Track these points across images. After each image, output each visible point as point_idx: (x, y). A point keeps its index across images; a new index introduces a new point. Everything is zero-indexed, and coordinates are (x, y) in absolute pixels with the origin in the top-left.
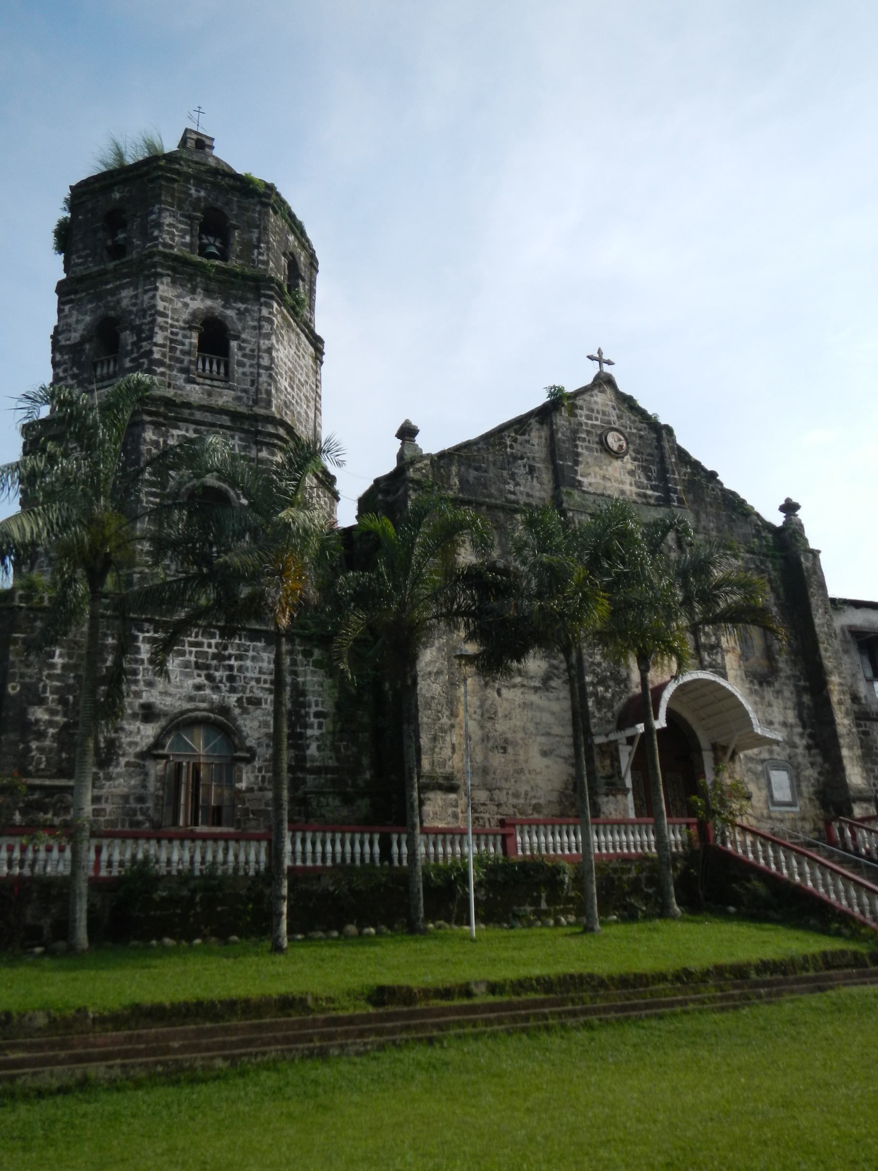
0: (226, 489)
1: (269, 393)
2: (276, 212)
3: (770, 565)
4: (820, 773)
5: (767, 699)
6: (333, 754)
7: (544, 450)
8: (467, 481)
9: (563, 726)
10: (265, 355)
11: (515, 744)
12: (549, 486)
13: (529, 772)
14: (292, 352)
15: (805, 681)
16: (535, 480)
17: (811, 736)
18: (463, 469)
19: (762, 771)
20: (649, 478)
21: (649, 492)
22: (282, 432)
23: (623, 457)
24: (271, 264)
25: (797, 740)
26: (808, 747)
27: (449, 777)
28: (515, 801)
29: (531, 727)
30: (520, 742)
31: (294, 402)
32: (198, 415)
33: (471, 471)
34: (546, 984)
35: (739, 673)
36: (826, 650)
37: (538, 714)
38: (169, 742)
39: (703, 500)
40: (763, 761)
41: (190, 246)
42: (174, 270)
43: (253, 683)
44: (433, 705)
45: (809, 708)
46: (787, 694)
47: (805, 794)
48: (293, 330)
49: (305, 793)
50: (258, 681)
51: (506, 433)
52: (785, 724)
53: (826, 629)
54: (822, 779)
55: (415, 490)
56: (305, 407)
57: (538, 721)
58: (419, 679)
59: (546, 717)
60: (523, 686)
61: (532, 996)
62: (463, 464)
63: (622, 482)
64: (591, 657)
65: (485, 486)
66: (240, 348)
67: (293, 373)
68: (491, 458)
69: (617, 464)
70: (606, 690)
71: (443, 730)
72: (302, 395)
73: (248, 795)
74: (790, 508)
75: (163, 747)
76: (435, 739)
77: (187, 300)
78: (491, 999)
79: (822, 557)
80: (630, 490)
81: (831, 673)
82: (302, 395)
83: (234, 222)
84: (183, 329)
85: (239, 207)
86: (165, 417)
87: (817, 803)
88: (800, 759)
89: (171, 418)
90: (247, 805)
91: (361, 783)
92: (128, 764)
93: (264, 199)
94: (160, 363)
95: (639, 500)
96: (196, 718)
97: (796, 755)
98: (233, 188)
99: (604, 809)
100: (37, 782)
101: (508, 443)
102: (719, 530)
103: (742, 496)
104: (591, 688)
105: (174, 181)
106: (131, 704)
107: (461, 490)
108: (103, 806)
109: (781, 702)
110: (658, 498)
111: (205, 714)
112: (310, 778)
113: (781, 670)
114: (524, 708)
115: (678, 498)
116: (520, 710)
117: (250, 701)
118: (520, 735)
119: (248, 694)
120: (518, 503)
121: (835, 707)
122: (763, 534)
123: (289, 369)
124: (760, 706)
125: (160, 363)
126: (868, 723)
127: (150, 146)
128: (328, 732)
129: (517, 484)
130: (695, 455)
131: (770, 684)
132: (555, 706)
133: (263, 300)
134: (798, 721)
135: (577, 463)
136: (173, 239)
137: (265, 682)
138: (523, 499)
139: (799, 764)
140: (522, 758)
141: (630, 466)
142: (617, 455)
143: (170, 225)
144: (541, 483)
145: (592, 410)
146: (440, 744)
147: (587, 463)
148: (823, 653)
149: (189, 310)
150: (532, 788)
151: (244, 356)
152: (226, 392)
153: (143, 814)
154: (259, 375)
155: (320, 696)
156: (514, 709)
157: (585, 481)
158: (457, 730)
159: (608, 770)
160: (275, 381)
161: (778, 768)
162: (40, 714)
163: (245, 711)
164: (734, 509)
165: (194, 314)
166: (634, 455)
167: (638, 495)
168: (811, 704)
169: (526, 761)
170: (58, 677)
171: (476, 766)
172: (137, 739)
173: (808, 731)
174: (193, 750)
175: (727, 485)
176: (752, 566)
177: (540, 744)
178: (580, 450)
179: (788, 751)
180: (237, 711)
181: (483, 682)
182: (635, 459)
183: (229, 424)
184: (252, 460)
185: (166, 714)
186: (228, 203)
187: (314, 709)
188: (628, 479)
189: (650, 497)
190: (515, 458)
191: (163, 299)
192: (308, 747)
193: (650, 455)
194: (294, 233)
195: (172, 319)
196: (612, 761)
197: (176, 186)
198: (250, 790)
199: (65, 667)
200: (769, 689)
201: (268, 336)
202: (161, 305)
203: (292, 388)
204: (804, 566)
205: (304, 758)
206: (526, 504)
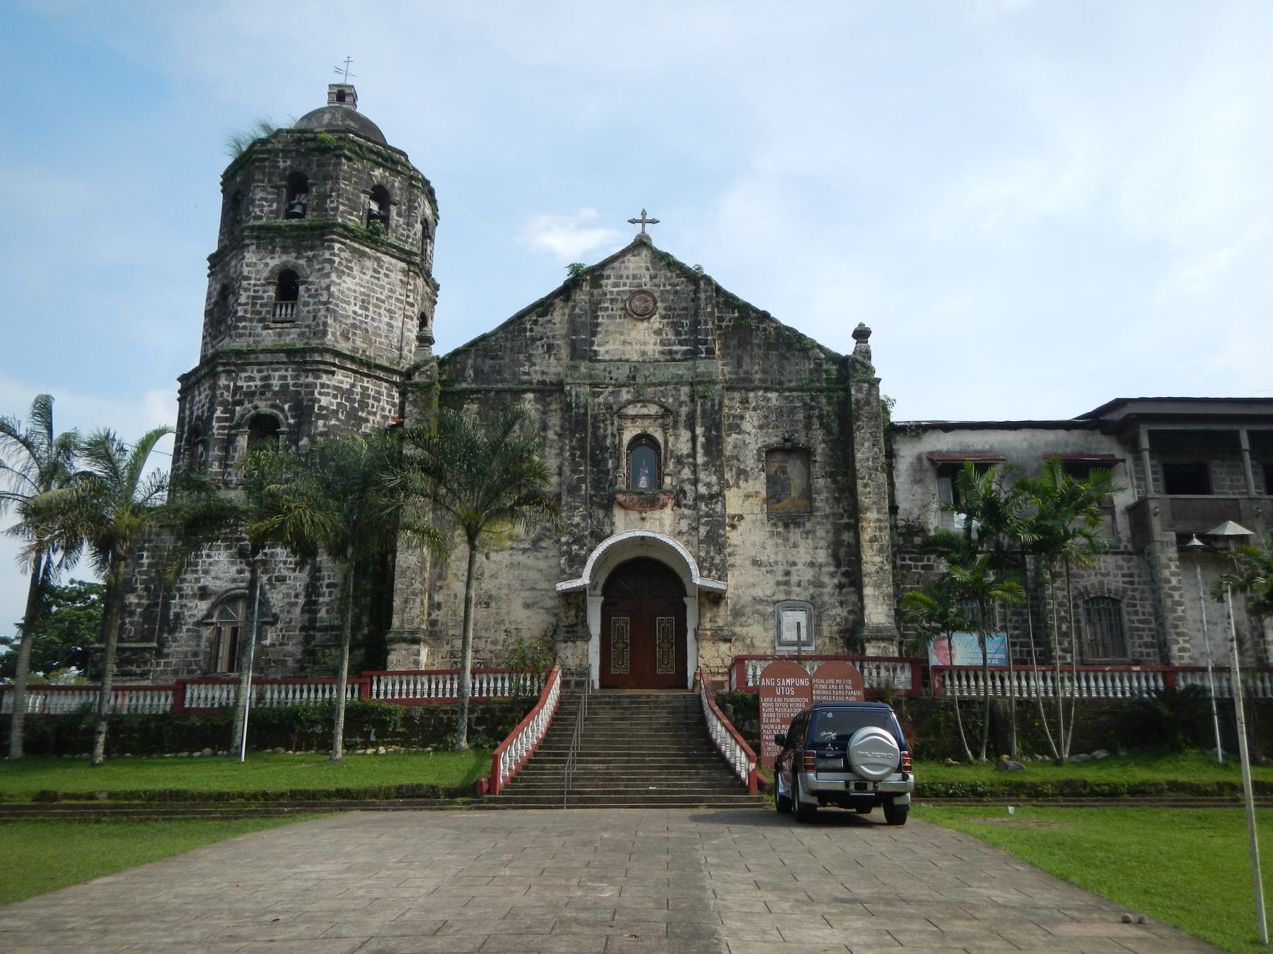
0: (277, 415)
1: (325, 324)
2: (349, 159)
3: (824, 401)
4: (850, 612)
5: (792, 541)
6: (339, 616)
7: (566, 326)
8: (482, 371)
9: (549, 581)
10: (325, 293)
11: (498, 599)
12: (565, 360)
13: (510, 623)
14: (368, 277)
15: (849, 518)
16: (552, 357)
17: (845, 574)
18: (479, 360)
20: (678, 333)
21: (675, 348)
22: (328, 358)
23: (650, 318)
24: (341, 208)
25: (826, 579)
26: (840, 586)
27: (412, 633)
28: (493, 648)
29: (517, 584)
30: (504, 597)
31: (368, 320)
32: (262, 357)
33: (486, 360)
34: (152, 796)
35: (759, 517)
36: (865, 486)
37: (525, 572)
38: (216, 614)
39: (750, 343)
40: (775, 603)
41: (277, 212)
42: (257, 238)
43: (281, 565)
44: (408, 573)
45: (849, 545)
46: (820, 532)
47: (826, 633)
48: (369, 257)
49: (315, 646)
50: (285, 563)
51: (527, 318)
52: (812, 564)
53: (870, 463)
54: (851, 617)
55: (413, 392)
56: (387, 320)
58: (398, 554)
59: (533, 575)
60: (512, 548)
61: (138, 802)
62: (479, 356)
63: (645, 344)
65: (499, 373)
66: (308, 290)
67: (369, 296)
68: (509, 345)
69: (643, 326)
70: (581, 548)
71: (414, 594)
72: (382, 311)
73: (271, 649)
74: (861, 334)
75: (212, 617)
76: (406, 601)
77: (268, 260)
78: (108, 802)
79: (881, 385)
80: (653, 348)
81: (867, 509)
82: (382, 311)
83: (310, 181)
84: (263, 285)
85: (318, 165)
86: (235, 364)
87: (840, 642)
88: (826, 598)
89: (239, 365)
90: (270, 656)
91: (360, 637)
92: (188, 630)
93: (338, 152)
94: (243, 319)
95: (662, 358)
96: (236, 594)
97: (821, 594)
98: (313, 150)
99: (561, 654)
100: (127, 645)
101: (529, 327)
102: (765, 372)
103: (800, 331)
105: (265, 159)
106: (187, 588)
107: (474, 381)
108: (171, 660)
109: (810, 541)
110: (685, 353)
111: (243, 591)
112: (318, 634)
113: (818, 509)
115: (706, 349)
117: (278, 579)
118: (504, 591)
119: (277, 574)
120: (531, 383)
121: (865, 545)
122: (825, 367)
123: (361, 294)
124: (782, 548)
125: (243, 319)
126: (933, 557)
127: (266, 127)
128: (337, 599)
129: (533, 364)
130: (744, 295)
131: (797, 525)
132: (543, 564)
133: (326, 244)
135: (594, 334)
136: (261, 211)
137: (291, 563)
138: (536, 378)
139: (824, 603)
140: (504, 611)
141: (657, 326)
142: (644, 315)
143: (262, 199)
144: (558, 360)
145: (621, 277)
147: (607, 331)
148: (860, 488)
149: (269, 268)
151: (309, 297)
152: (293, 330)
153: (196, 665)
154: (319, 310)
155: (333, 571)
156: (501, 569)
157: (602, 350)
158: (445, 591)
159: (572, 620)
160: (335, 311)
161: (793, 608)
162: (132, 599)
163: (273, 587)
164: (790, 346)
165: (272, 271)
166: (664, 312)
167: (662, 353)
168: (852, 541)
169: (508, 613)
170: (145, 573)
171: (459, 619)
172: (195, 612)
173: (843, 569)
174: (232, 617)
175: (785, 321)
176: (798, 405)
178: (600, 320)
180: (267, 587)
182: (664, 317)
183: (285, 360)
184: (301, 385)
185: (215, 594)
186: (309, 165)
187: (326, 581)
188: (653, 339)
189: (676, 352)
190: (533, 340)
191: (247, 266)
192: (319, 611)
193: (685, 309)
194: (379, 165)
195: (256, 279)
196: (577, 611)
197: (267, 164)
198: (273, 645)
199: (150, 565)
201: (328, 275)
202: (246, 271)
203: (367, 309)
204: (853, 399)
205: (315, 620)
206: (539, 382)
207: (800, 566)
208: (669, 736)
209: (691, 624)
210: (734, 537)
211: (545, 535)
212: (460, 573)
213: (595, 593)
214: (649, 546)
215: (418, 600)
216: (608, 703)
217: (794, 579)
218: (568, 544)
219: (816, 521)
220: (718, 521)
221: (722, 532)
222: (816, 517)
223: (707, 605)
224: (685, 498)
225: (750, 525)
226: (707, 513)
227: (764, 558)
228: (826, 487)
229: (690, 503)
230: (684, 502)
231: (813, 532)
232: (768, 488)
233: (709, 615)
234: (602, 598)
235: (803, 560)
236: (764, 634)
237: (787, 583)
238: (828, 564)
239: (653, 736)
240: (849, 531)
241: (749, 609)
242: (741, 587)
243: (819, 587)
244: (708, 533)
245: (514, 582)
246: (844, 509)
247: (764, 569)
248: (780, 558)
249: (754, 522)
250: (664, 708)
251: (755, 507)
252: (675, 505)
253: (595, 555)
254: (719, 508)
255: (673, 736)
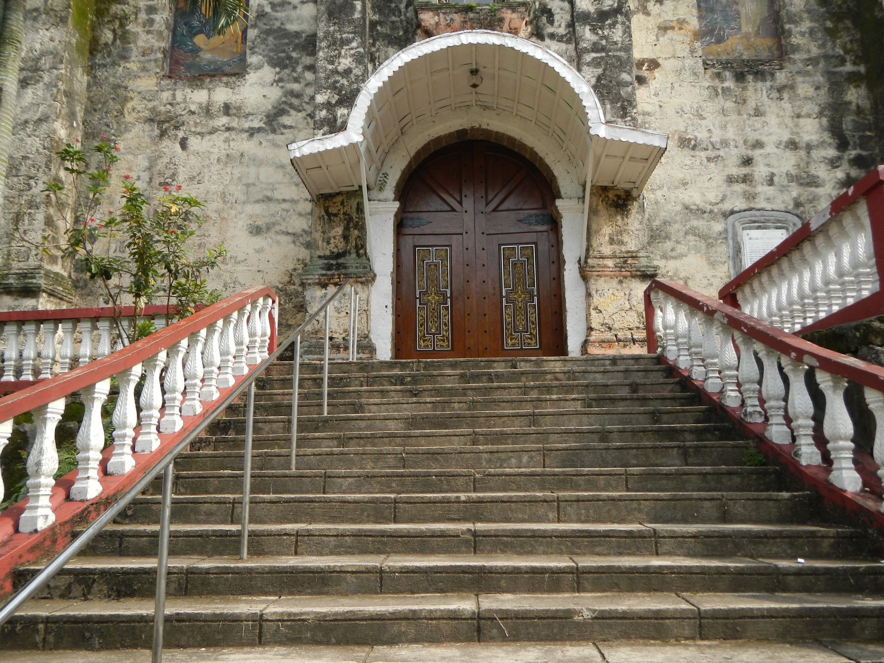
5: (752, 104)
15: (855, 64)
17: (857, 162)
19: (726, 230)
25: (821, 171)
29: (237, 192)
30: (214, 215)
35: (689, 62)
37: (252, 170)
44: (23, 168)
45: (859, 111)
46: (804, 88)
52: (793, 145)
57: (251, 181)
59: (268, 175)
64: (332, 63)
71: (32, 204)
104: (324, 113)
109: (786, 105)
113: (796, 49)
114: (226, 163)
116: (221, 166)
124: (734, 117)
131: (760, 75)
134: (827, 137)
140: (213, 239)
146: (24, 225)
150: (225, 286)
159: (337, 245)
161: (761, 225)
168: (866, 104)
173: (853, 153)
177: (251, 216)
179: (794, 194)
181: (157, 132)
196: (347, 228)
200: (760, 84)
207: (770, 149)
208: (627, 482)
209: (572, 250)
210: (644, 97)
211: (291, 106)
212: (134, 175)
213: (382, 196)
214: (486, 108)
215: (40, 216)
216: (401, 380)
217: (760, 171)
218: (328, 106)
219: (794, 68)
220: (619, 59)
221: (625, 77)
222: (794, 62)
223: (601, 207)
224: (551, 22)
225: (672, 78)
226: (595, 44)
227: (702, 135)
228: (809, 11)
229: (562, 31)
230: (550, 30)
231: (792, 87)
232: (700, 18)
233: (607, 230)
234: (397, 204)
235: (774, 138)
236: (709, 274)
237: (746, 179)
238: (822, 144)
239: (564, 482)
240: (856, 87)
241: (676, 226)
242: (660, 188)
243: (809, 184)
244: (599, 79)
245: (232, 188)
246: (844, 48)
247: (703, 154)
248: (731, 133)
249: (679, 72)
250: (570, 389)
251: (679, 47)
252: (532, 35)
253: (375, 83)
254: (617, 35)
255: (648, 480)
